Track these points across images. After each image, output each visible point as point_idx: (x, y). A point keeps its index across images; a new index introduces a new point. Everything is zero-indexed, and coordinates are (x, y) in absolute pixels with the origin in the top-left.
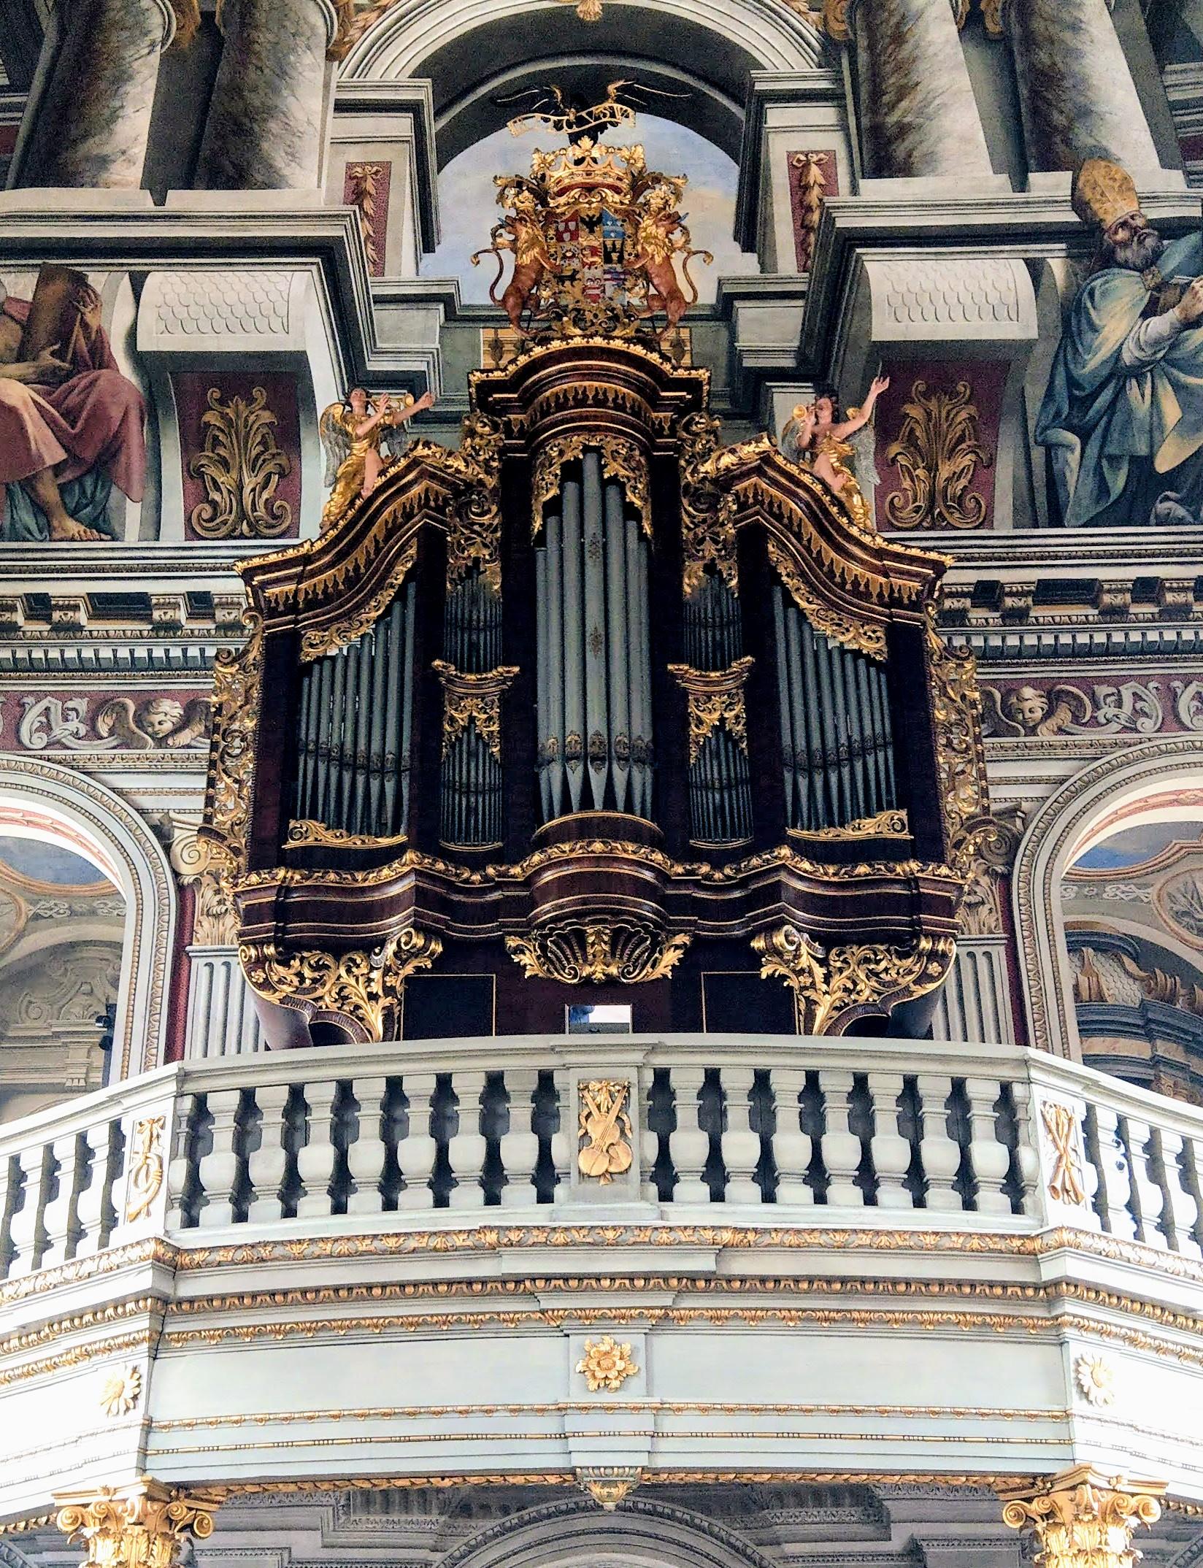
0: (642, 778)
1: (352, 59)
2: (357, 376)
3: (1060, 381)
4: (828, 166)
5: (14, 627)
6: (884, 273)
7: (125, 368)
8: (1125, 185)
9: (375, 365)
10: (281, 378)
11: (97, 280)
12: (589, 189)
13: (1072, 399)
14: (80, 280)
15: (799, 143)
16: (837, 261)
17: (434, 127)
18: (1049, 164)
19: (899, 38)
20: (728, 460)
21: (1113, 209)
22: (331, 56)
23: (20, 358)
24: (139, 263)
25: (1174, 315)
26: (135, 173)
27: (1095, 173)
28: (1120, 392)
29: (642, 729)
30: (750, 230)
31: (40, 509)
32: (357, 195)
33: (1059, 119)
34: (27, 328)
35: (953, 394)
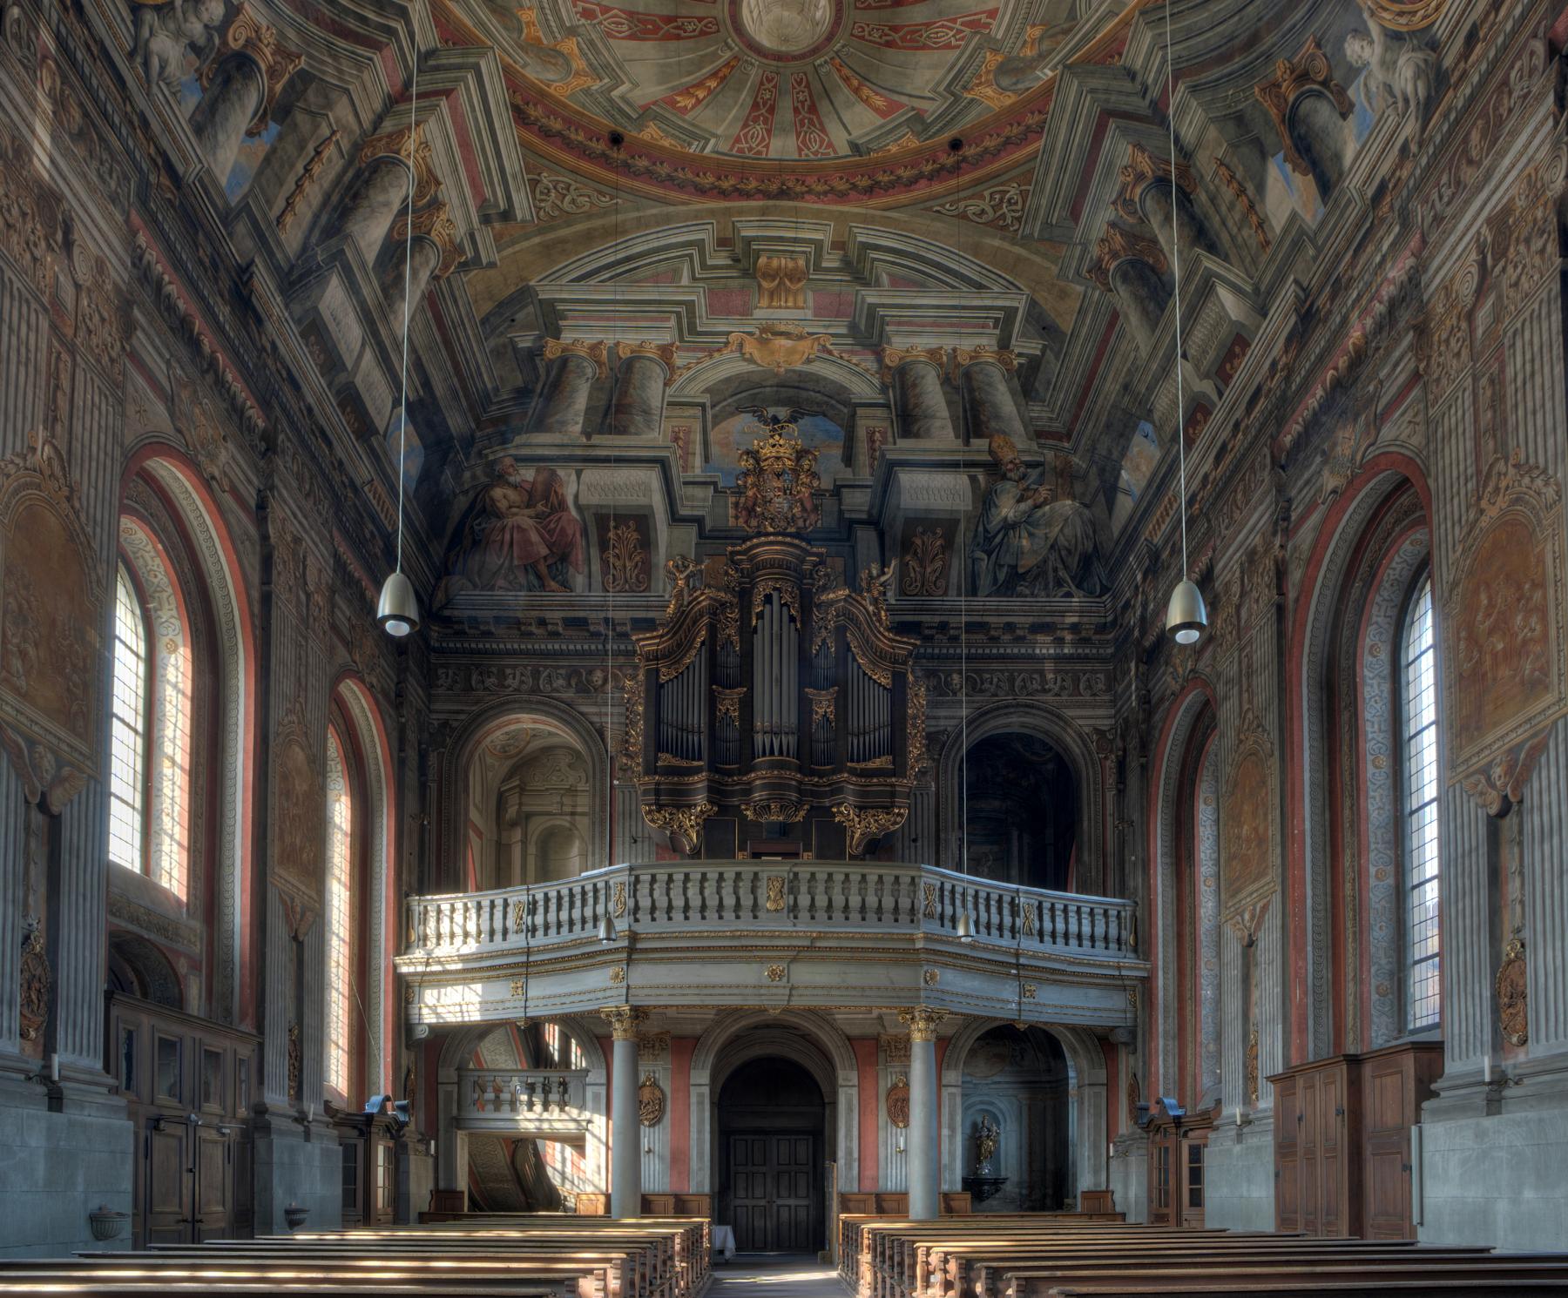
0: (793, 740)
1: (675, 386)
2: (675, 519)
3: (981, 529)
4: (883, 434)
5: (531, 634)
6: (906, 478)
7: (574, 512)
8: (1013, 447)
9: (684, 512)
10: (641, 520)
11: (561, 473)
12: (778, 458)
13: (985, 538)
14: (553, 473)
15: (871, 423)
16: (888, 472)
17: (710, 413)
18: (979, 435)
19: (914, 385)
20: (831, 596)
21: (1007, 456)
22: (665, 385)
23: (528, 506)
24: (579, 465)
25: (1030, 502)
26: (578, 428)
27: (998, 441)
28: (1006, 535)
29: (794, 720)
30: (849, 459)
31: (539, 577)
32: (676, 439)
33: (983, 418)
34: (530, 493)
35: (935, 534)
